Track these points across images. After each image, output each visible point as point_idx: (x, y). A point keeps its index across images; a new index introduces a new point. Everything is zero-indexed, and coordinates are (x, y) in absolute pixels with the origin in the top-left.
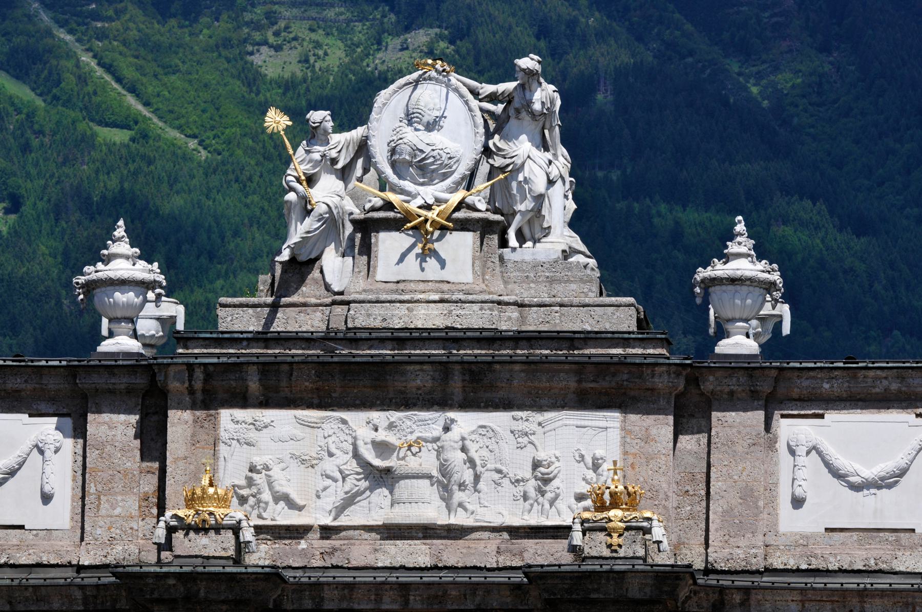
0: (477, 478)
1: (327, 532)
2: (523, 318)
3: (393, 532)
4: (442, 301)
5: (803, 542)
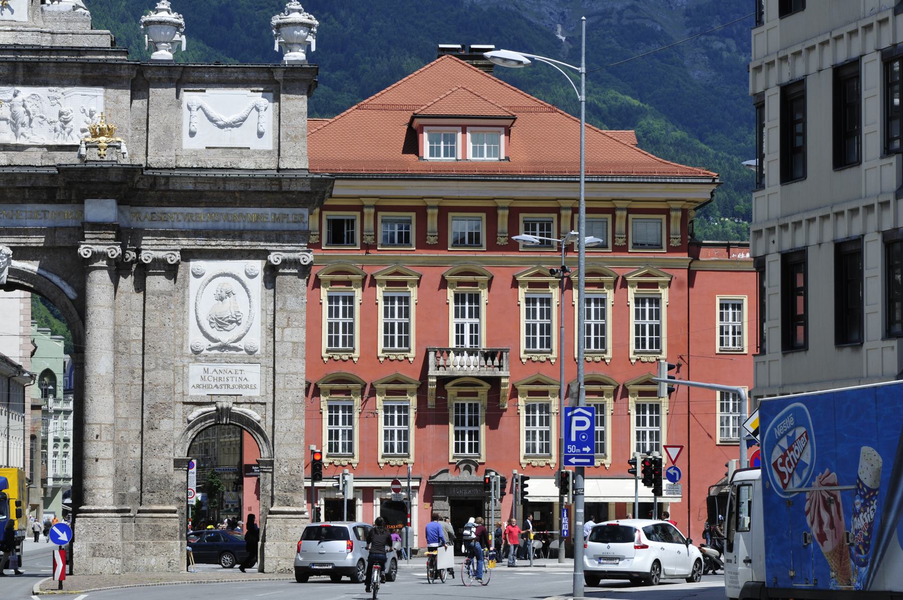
0: (31, 120)
2: (53, 40)
4: (12, 31)
5: (195, 153)
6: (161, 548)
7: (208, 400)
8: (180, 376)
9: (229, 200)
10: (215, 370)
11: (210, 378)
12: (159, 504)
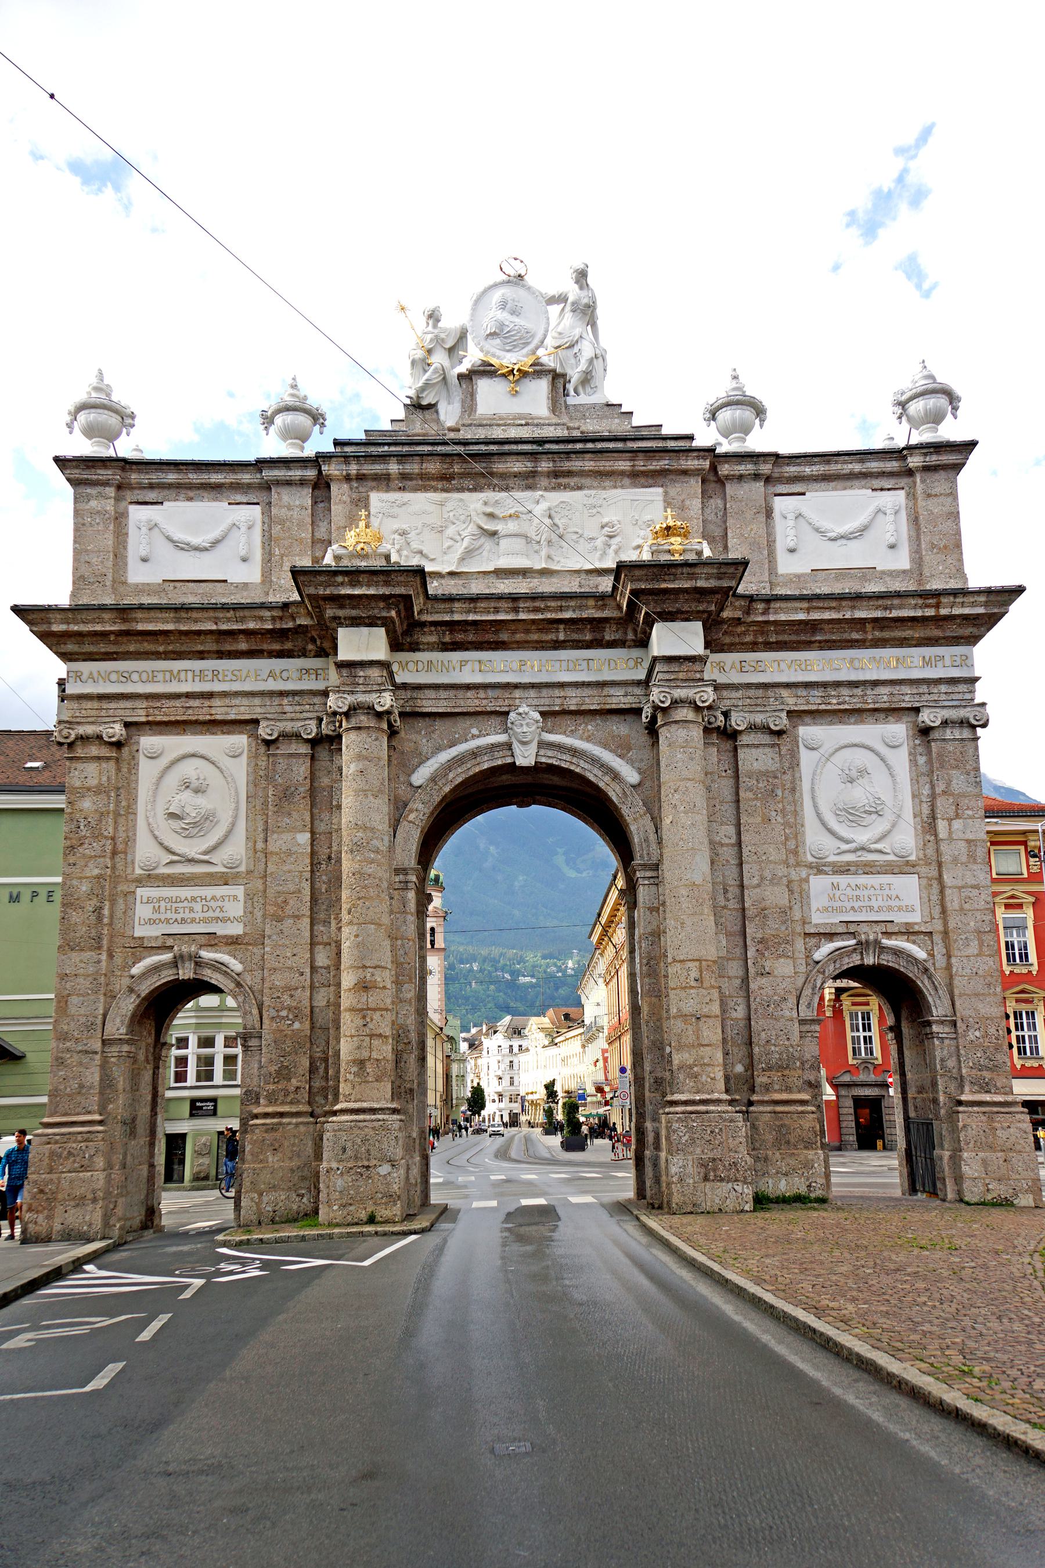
1: (452, 574)
3: (501, 573)
4: (527, 424)
6: (792, 1162)
7: (841, 929)
8: (796, 895)
9: (855, 636)
10: (849, 885)
12: (780, 1091)
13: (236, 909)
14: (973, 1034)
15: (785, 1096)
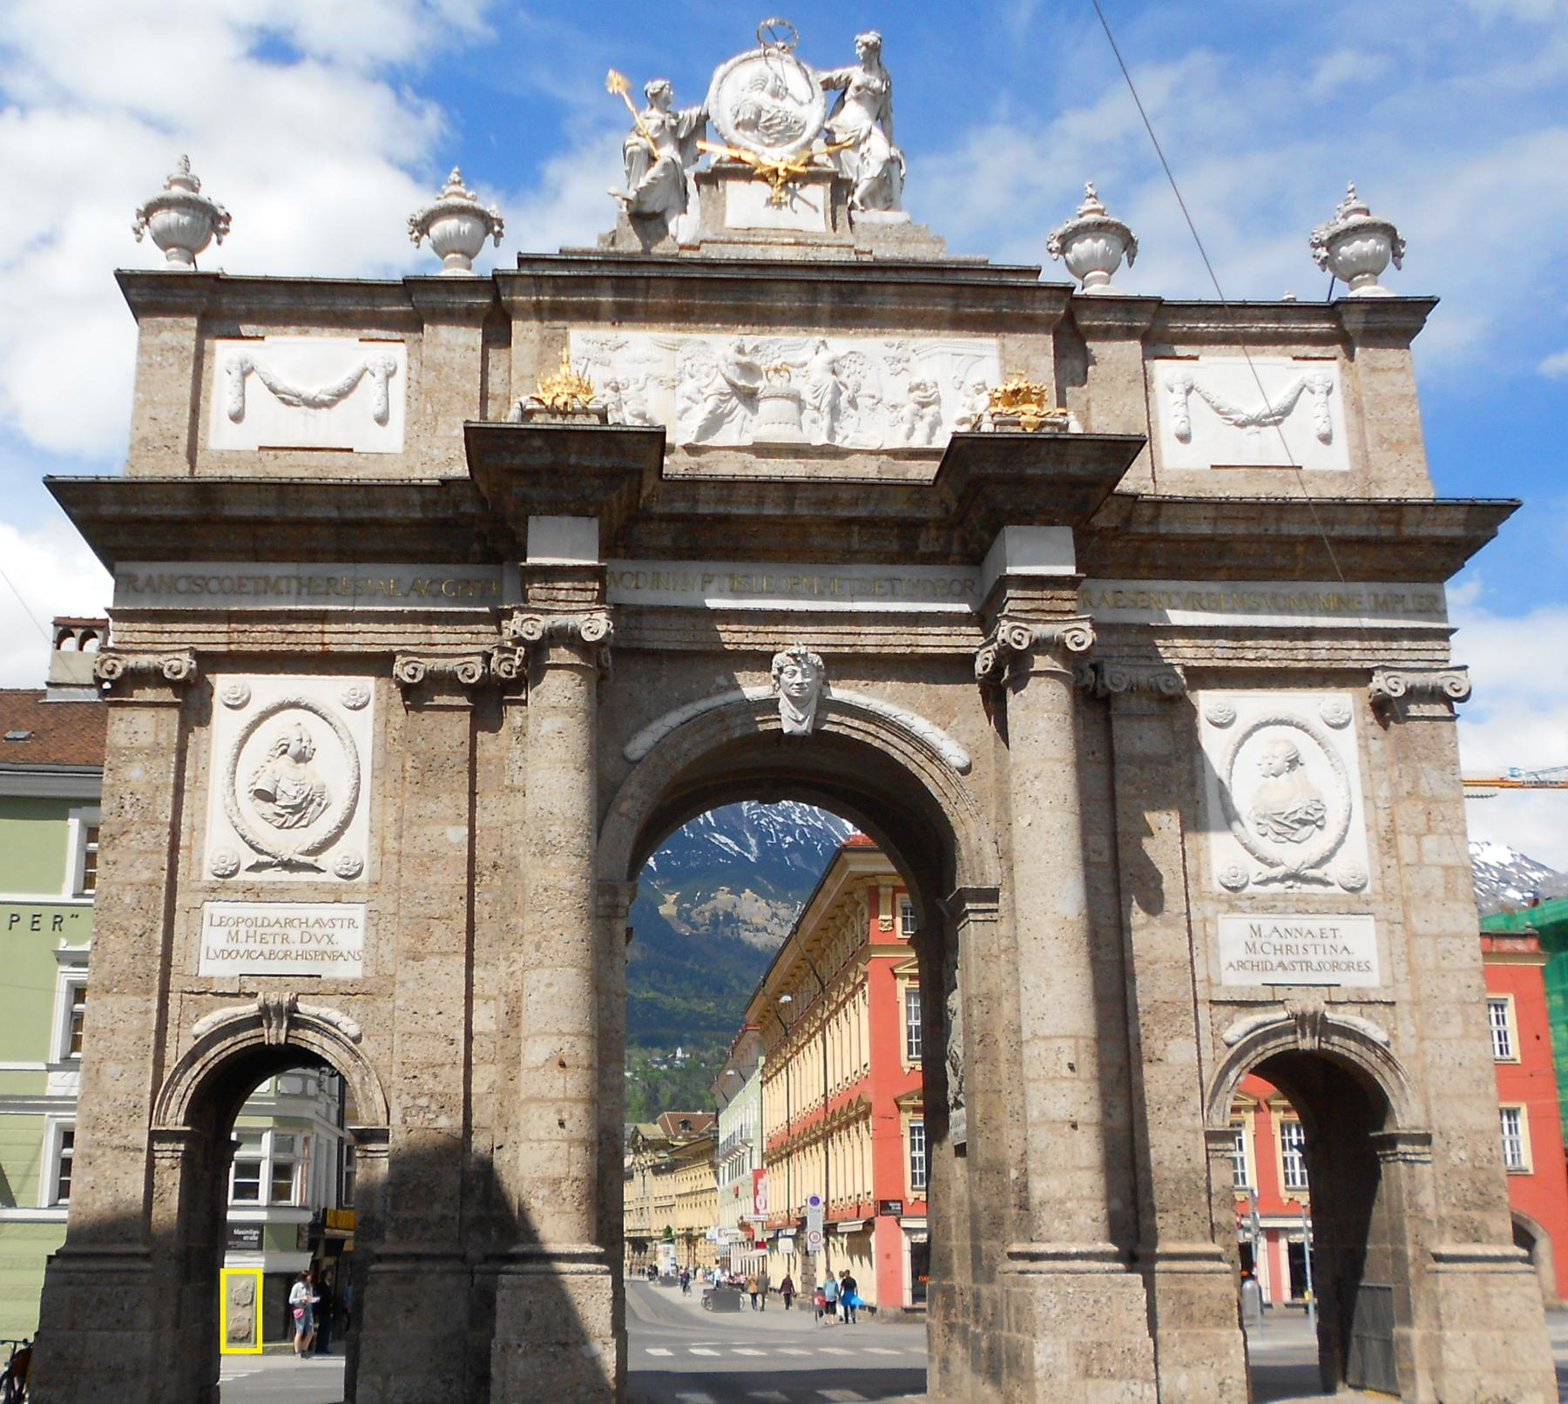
5: (1192, 476)
7: (1265, 995)
9: (1280, 561)
10: (1276, 930)
11: (1266, 948)
12: (1179, 1239)
13: (351, 939)
14: (1458, 1155)
15: (1185, 1248)
